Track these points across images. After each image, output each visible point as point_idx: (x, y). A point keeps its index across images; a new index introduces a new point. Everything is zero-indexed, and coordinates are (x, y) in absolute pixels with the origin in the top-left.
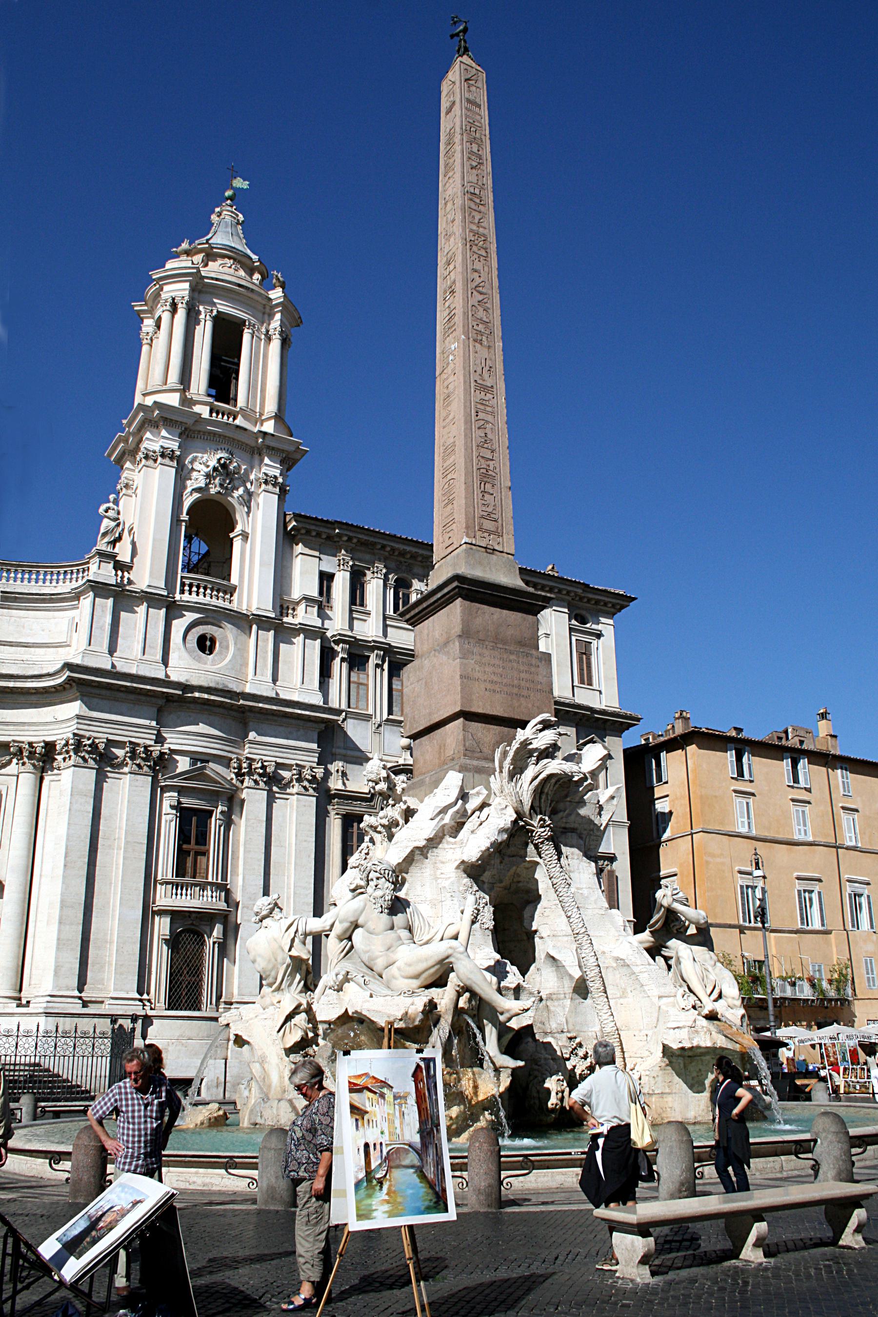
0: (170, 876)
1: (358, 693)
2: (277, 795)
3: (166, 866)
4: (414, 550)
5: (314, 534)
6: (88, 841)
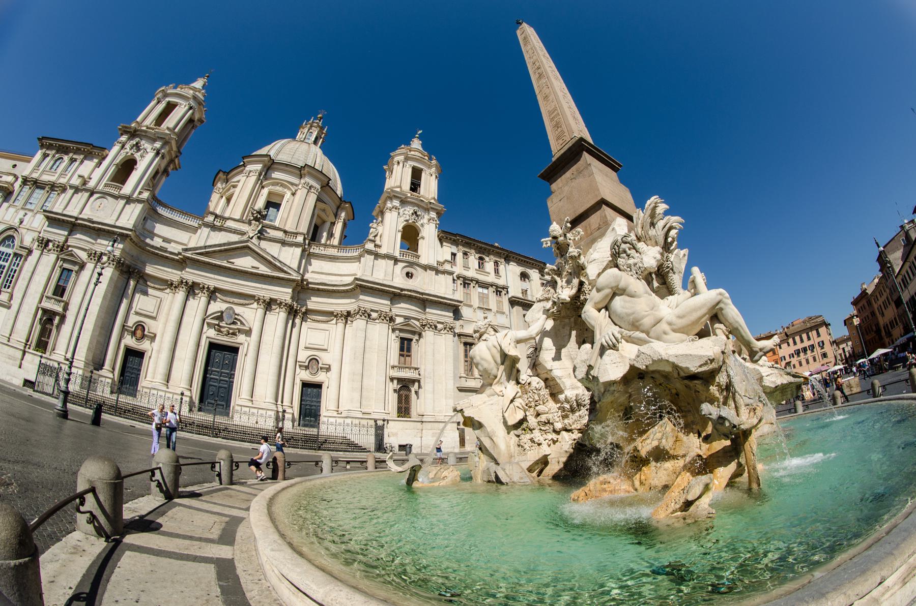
4: (485, 246)
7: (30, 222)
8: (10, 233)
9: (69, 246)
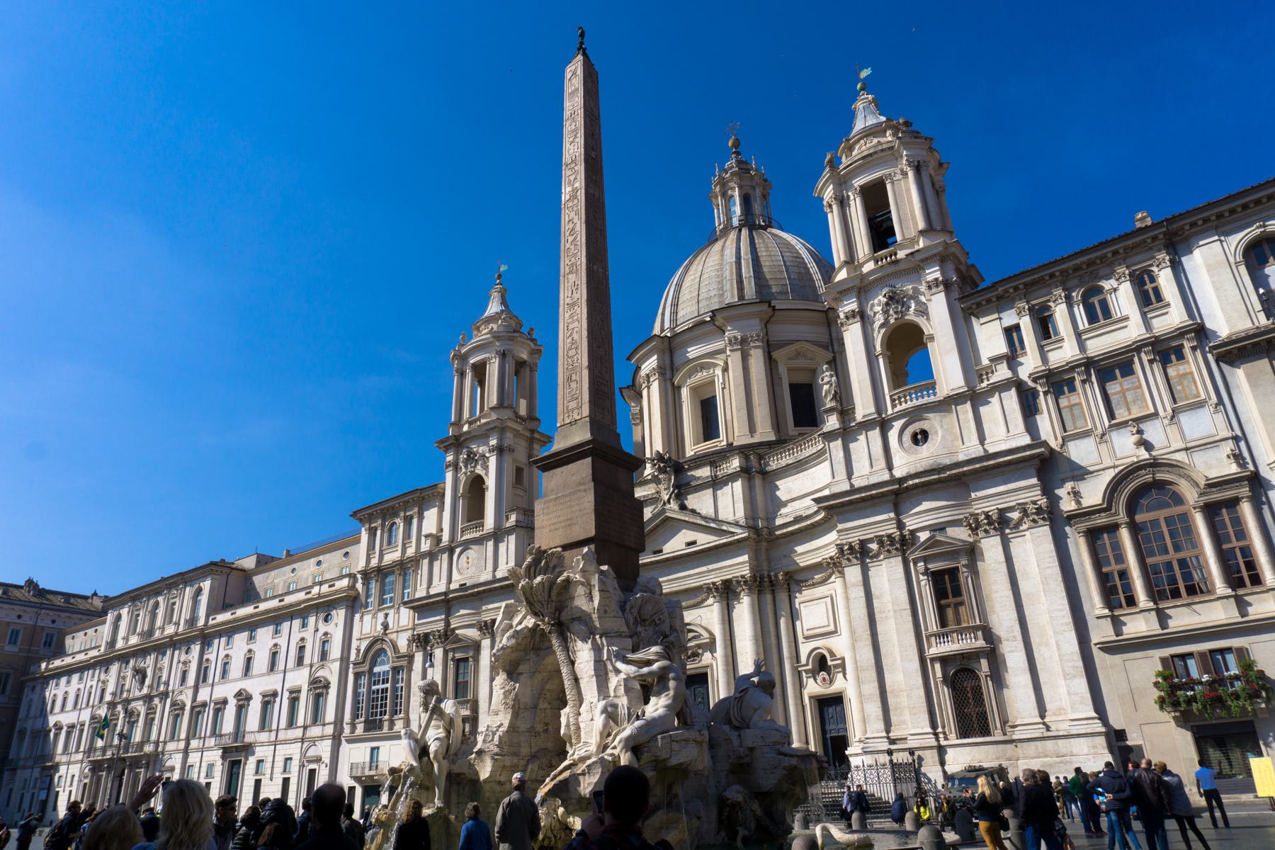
0: (935, 629)
1: (1073, 415)
2: (1010, 536)
3: (932, 624)
4: (1085, 258)
5: (984, 303)
6: (867, 618)
7: (396, 623)
8: (378, 646)
9: (454, 630)
